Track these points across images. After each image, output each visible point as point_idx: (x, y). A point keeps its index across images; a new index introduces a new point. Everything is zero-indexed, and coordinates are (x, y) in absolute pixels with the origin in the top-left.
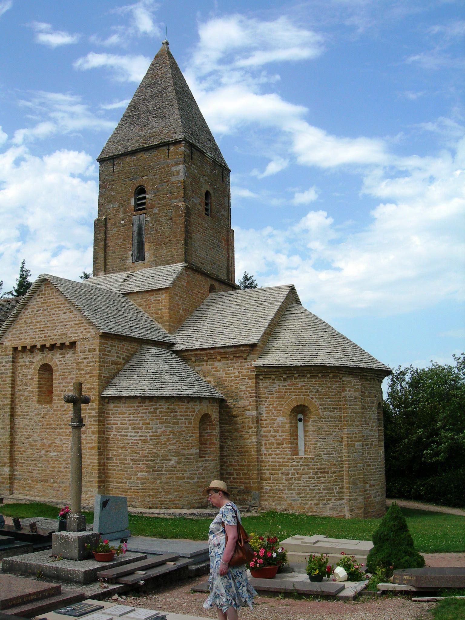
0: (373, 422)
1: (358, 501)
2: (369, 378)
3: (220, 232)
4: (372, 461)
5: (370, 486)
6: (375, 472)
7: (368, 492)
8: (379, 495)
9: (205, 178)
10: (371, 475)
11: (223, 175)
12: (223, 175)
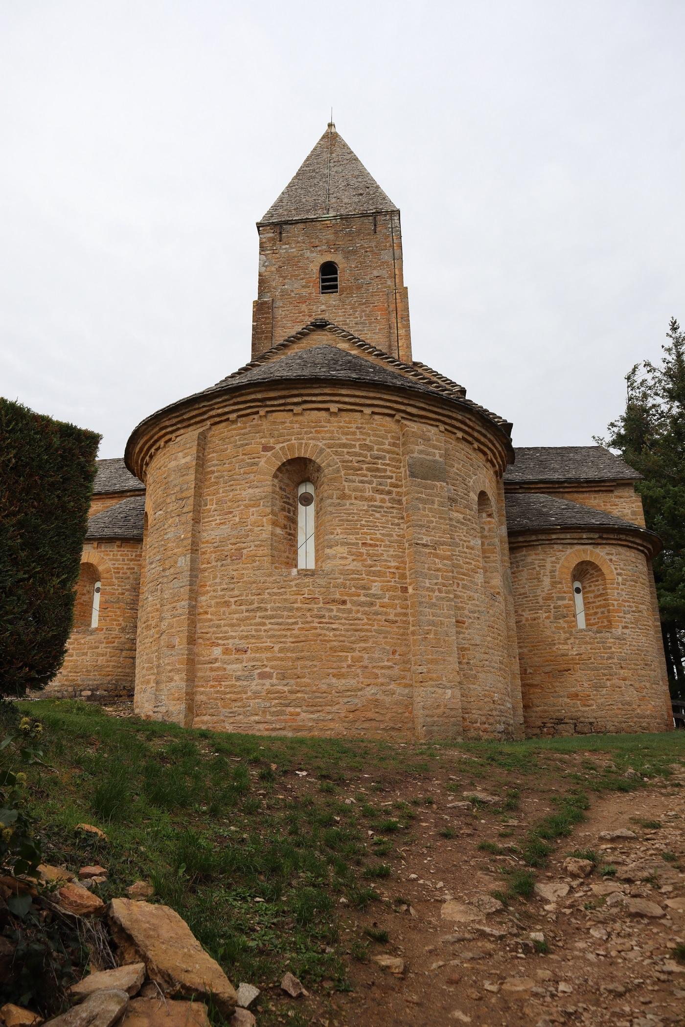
0: (247, 507)
1: (173, 684)
2: (233, 416)
3: (365, 304)
4: (236, 592)
5: (226, 651)
6: (247, 618)
7: (217, 665)
8: (262, 676)
9: (319, 248)
10: (232, 625)
11: (375, 225)
12: (375, 225)
